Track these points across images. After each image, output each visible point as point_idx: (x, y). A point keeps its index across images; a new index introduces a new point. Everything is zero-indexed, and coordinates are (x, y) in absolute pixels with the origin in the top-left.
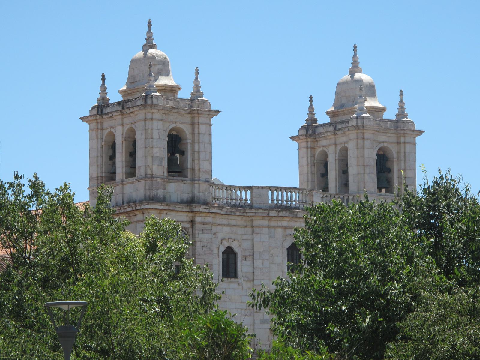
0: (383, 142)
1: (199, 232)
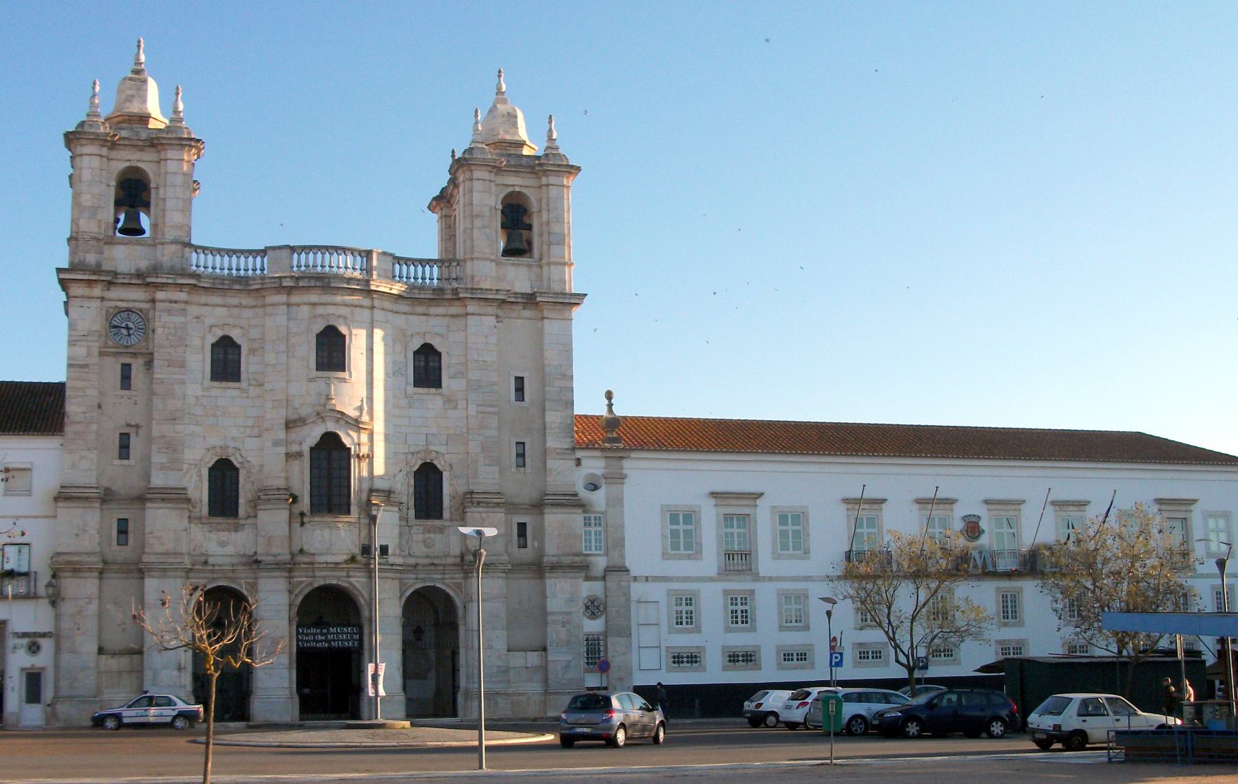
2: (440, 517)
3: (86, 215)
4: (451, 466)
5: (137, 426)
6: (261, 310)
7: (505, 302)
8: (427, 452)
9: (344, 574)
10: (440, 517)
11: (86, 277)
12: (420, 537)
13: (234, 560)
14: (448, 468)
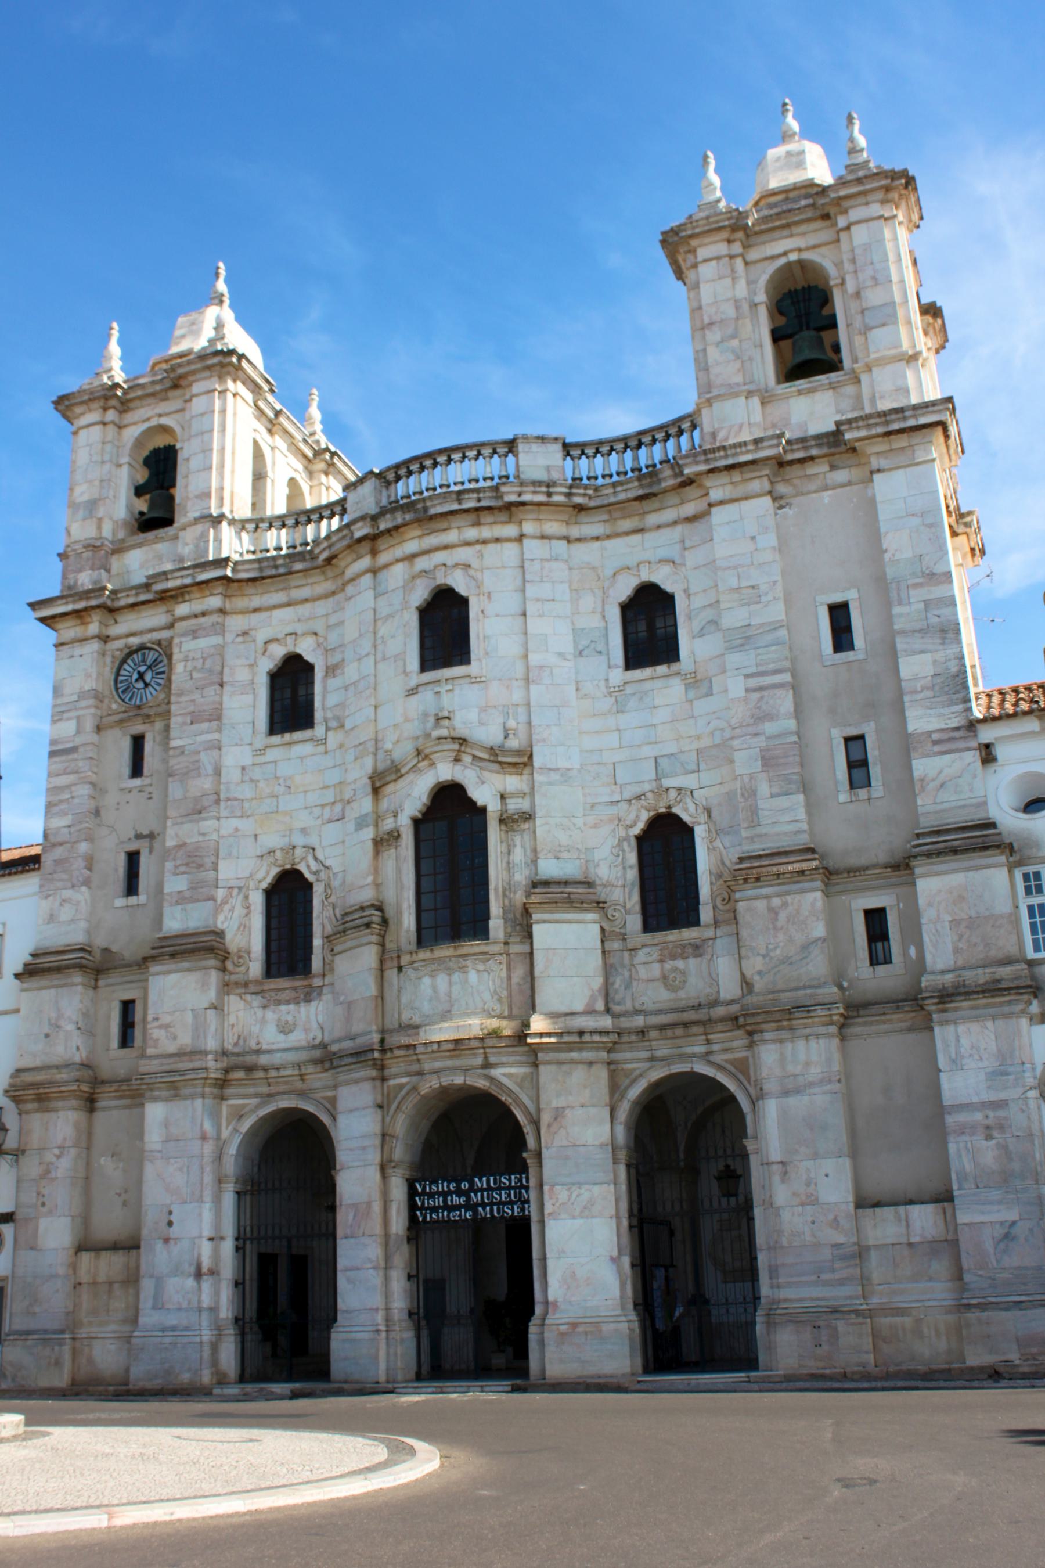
0: (785, 254)
1: (183, 639)
2: (696, 922)
3: (81, 514)
4: (709, 812)
5: (151, 836)
6: (340, 597)
7: (784, 465)
9: (479, 1061)
10: (696, 922)
12: (656, 970)
13: (303, 1056)
14: (703, 818)
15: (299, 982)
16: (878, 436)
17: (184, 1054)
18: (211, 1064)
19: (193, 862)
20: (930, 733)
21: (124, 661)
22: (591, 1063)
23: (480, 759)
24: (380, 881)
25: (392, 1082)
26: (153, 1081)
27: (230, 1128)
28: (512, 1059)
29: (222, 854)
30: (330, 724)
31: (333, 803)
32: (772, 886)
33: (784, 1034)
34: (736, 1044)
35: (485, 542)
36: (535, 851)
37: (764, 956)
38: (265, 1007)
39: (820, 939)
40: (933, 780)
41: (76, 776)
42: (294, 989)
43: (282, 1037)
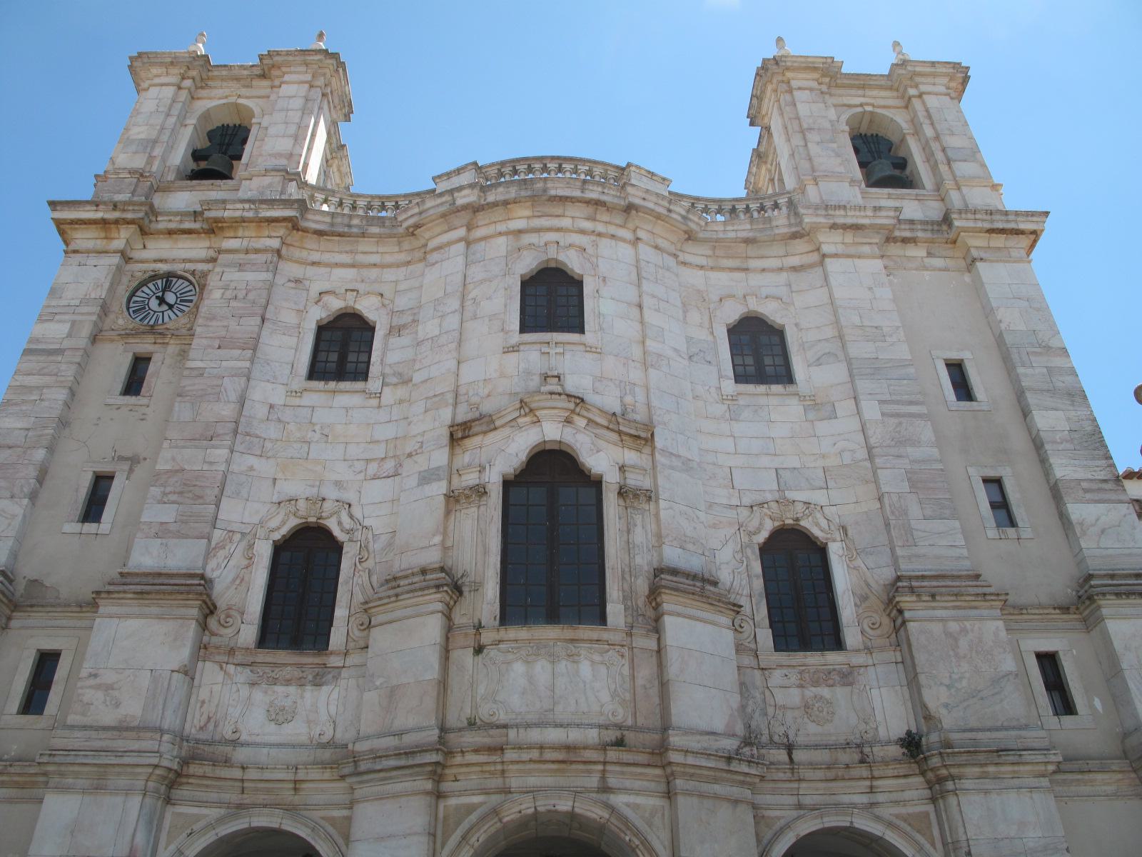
2: (837, 643)
4: (844, 529)
5: (134, 461)
8: (784, 502)
9: (594, 781)
10: (838, 644)
11: (99, 215)
12: (793, 697)
15: (309, 659)
16: (981, 231)
17: (128, 729)
18: (165, 747)
19: (190, 491)
20: (1079, 481)
21: (144, 283)
22: (736, 802)
23: (597, 424)
24: (449, 544)
25: (452, 802)
26: (69, 760)
27: (172, 847)
28: (638, 784)
29: (228, 491)
30: (387, 380)
31: (382, 459)
32: (946, 608)
33: (988, 784)
34: (908, 795)
35: (600, 235)
36: (659, 536)
37: (947, 686)
38: (253, 684)
39: (1010, 673)
40: (1093, 525)
41: (54, 378)
42: (300, 666)
43: (272, 727)
